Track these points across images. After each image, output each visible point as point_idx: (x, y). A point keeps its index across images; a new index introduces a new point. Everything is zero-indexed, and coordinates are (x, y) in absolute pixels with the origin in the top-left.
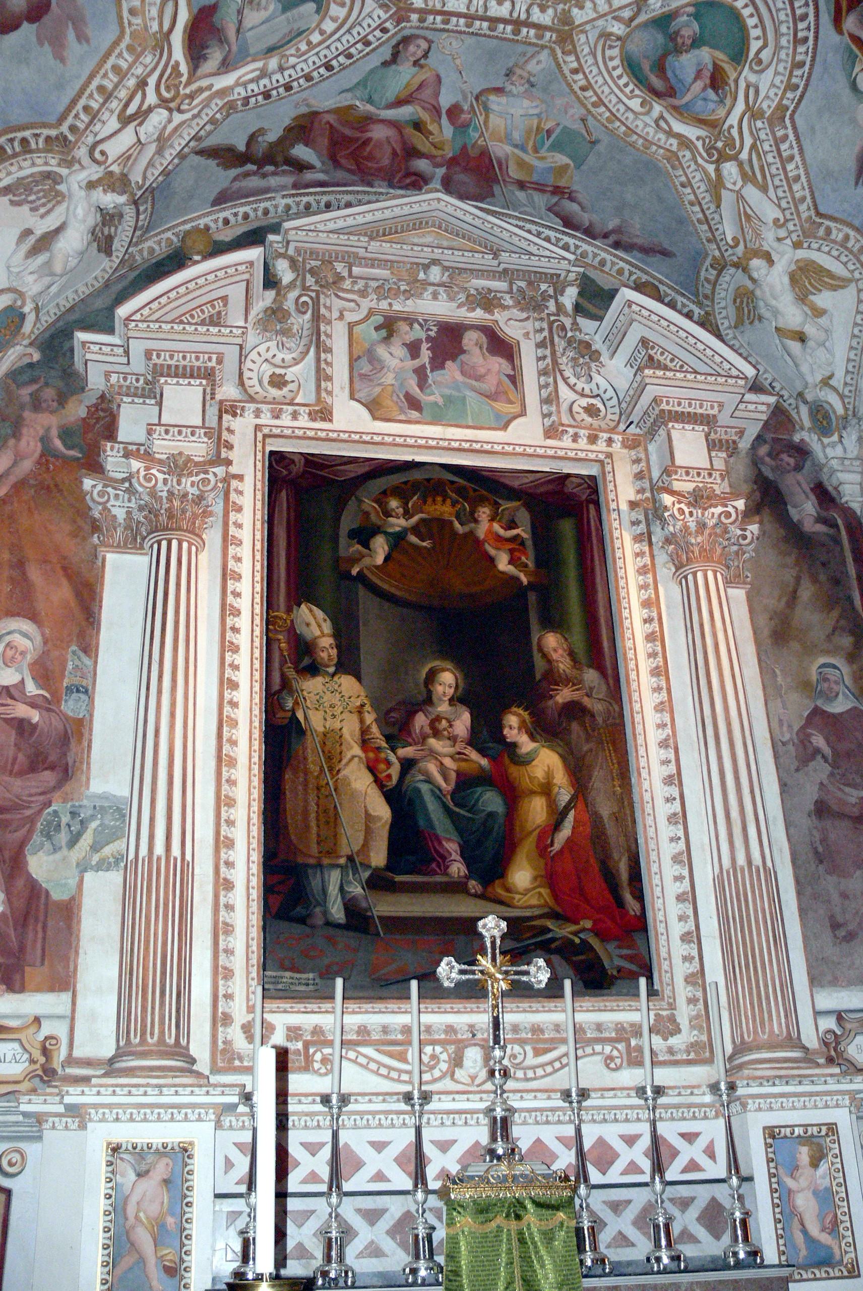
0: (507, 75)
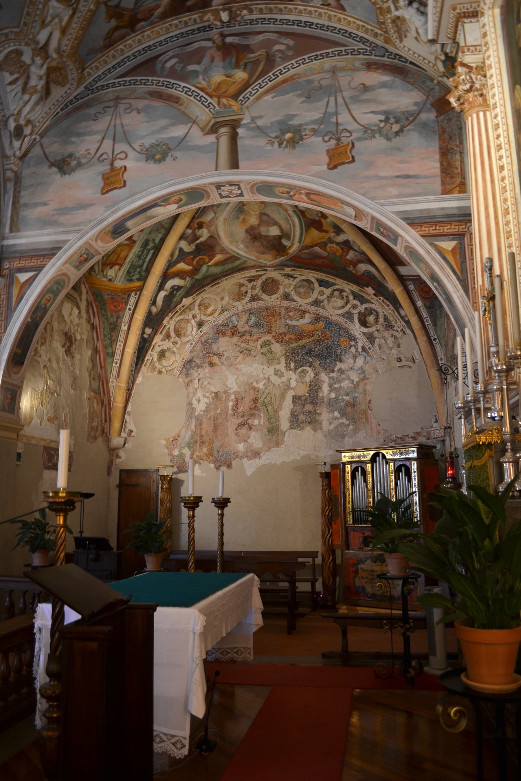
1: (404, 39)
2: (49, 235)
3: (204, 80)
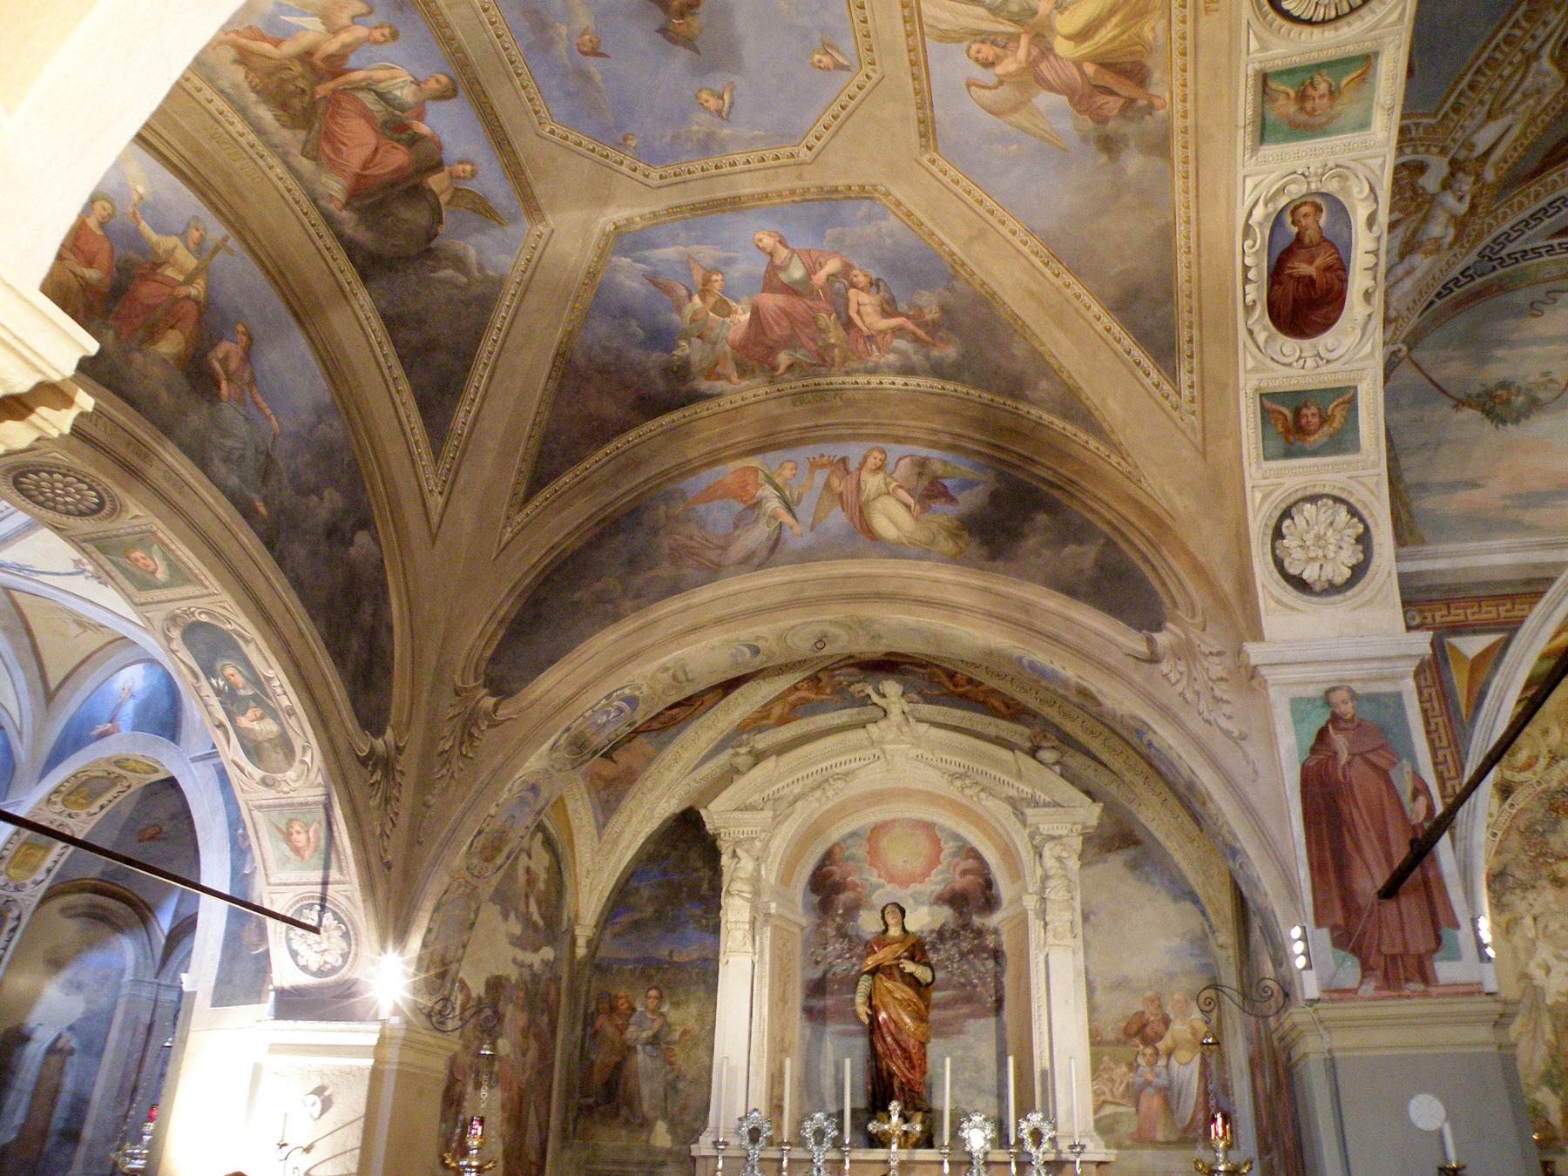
2: (1508, 550)
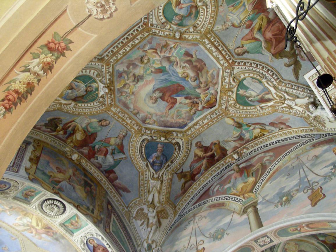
0: (228, 28)
1: (325, 125)
3: (234, 189)
